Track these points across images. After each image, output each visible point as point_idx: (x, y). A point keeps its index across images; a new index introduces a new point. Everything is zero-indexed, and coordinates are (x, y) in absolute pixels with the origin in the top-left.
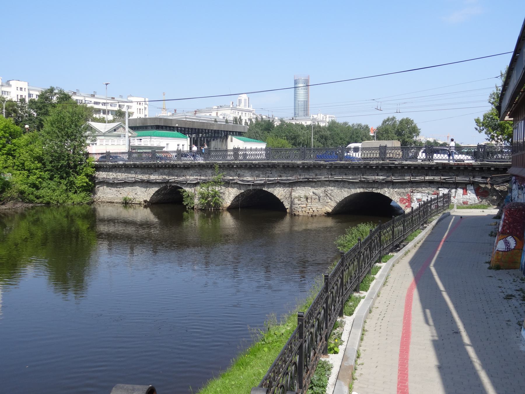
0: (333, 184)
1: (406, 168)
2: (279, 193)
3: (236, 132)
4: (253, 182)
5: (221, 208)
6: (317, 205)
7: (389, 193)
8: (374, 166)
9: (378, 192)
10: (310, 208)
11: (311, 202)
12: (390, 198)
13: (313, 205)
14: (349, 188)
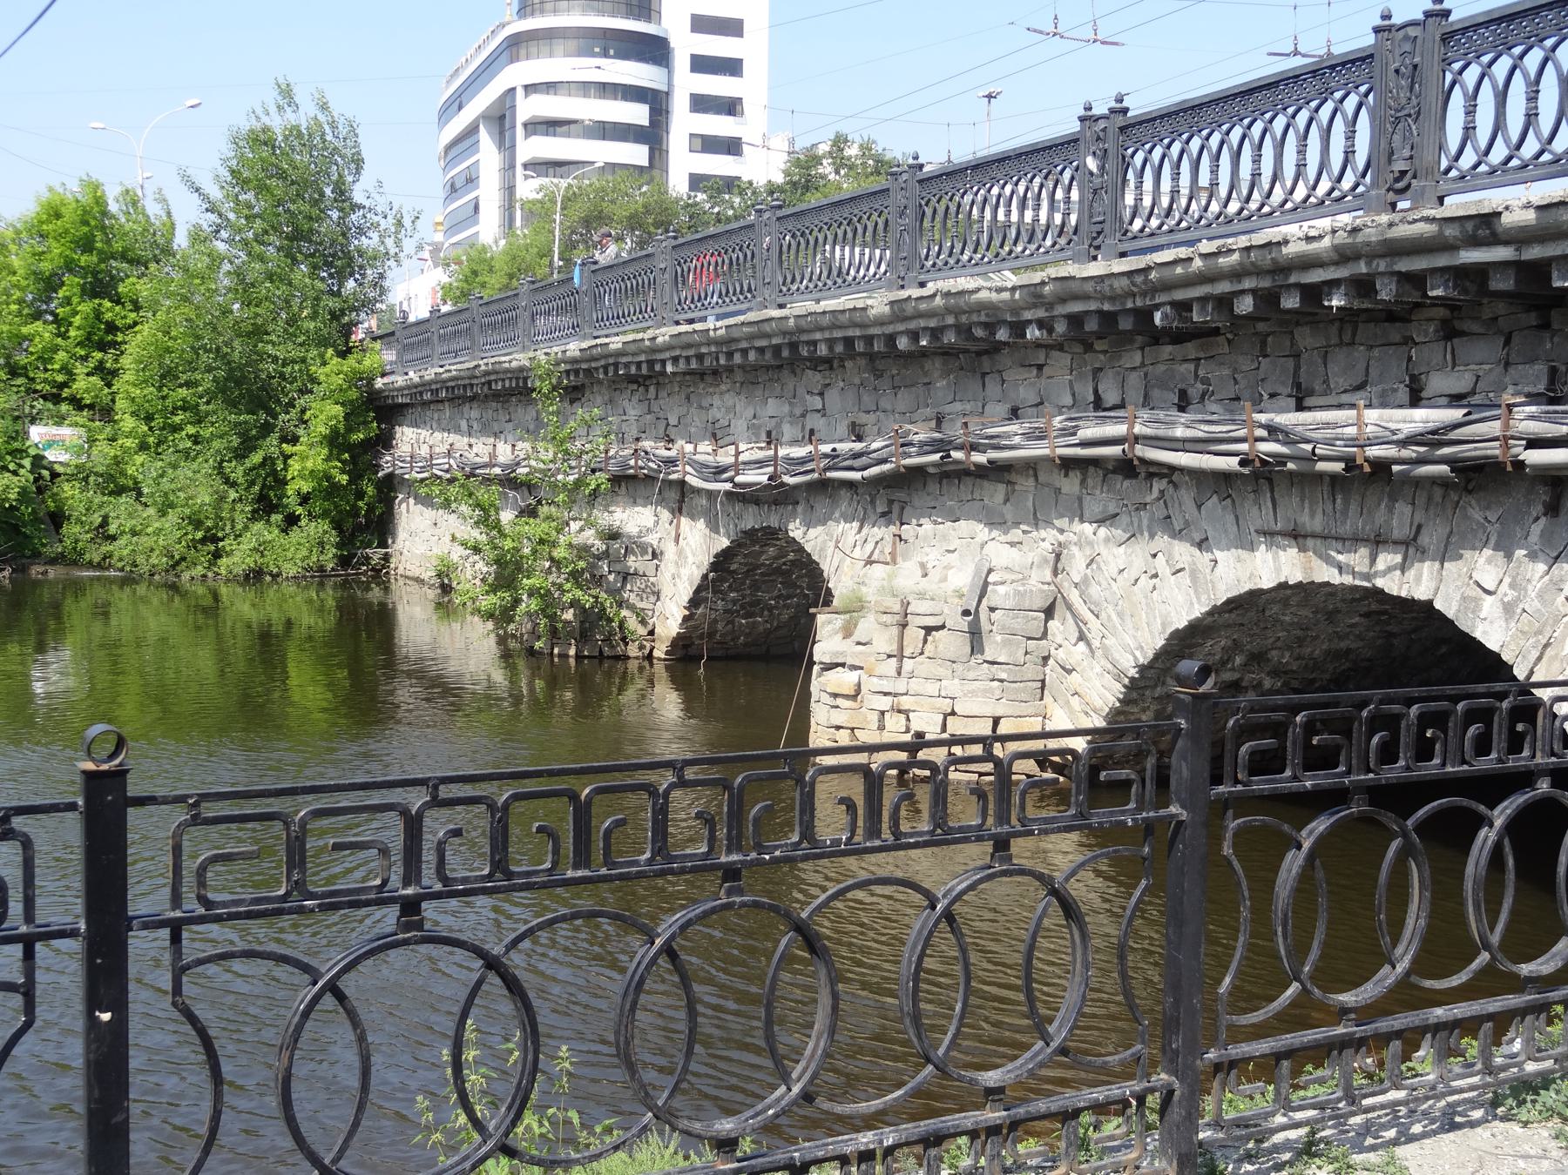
0: (1100, 500)
4: (731, 480)
5: (633, 651)
6: (952, 686)
7: (1508, 609)
8: (1333, 284)
9: (1421, 594)
10: (884, 703)
13: (915, 685)
14: (1202, 544)
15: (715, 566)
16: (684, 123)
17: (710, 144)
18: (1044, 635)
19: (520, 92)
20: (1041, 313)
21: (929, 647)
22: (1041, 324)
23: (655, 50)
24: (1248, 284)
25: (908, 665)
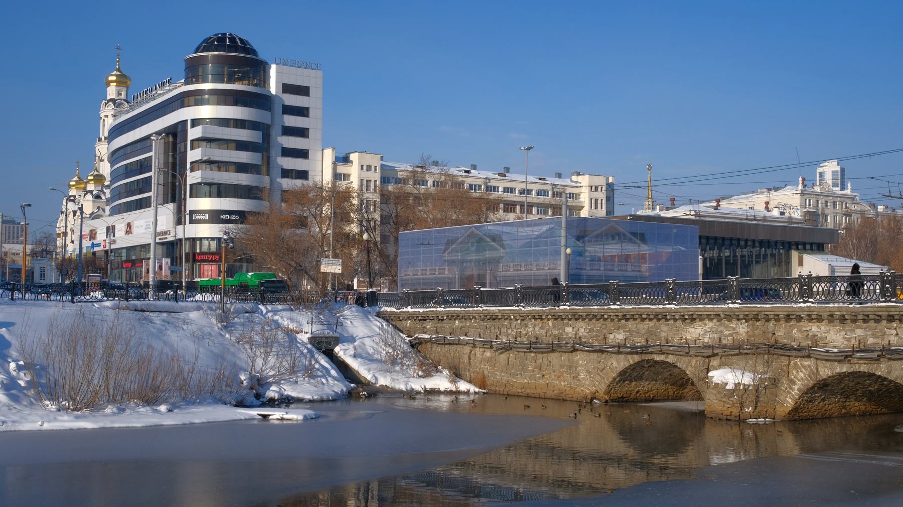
3: (811, 244)
23: (261, 101)
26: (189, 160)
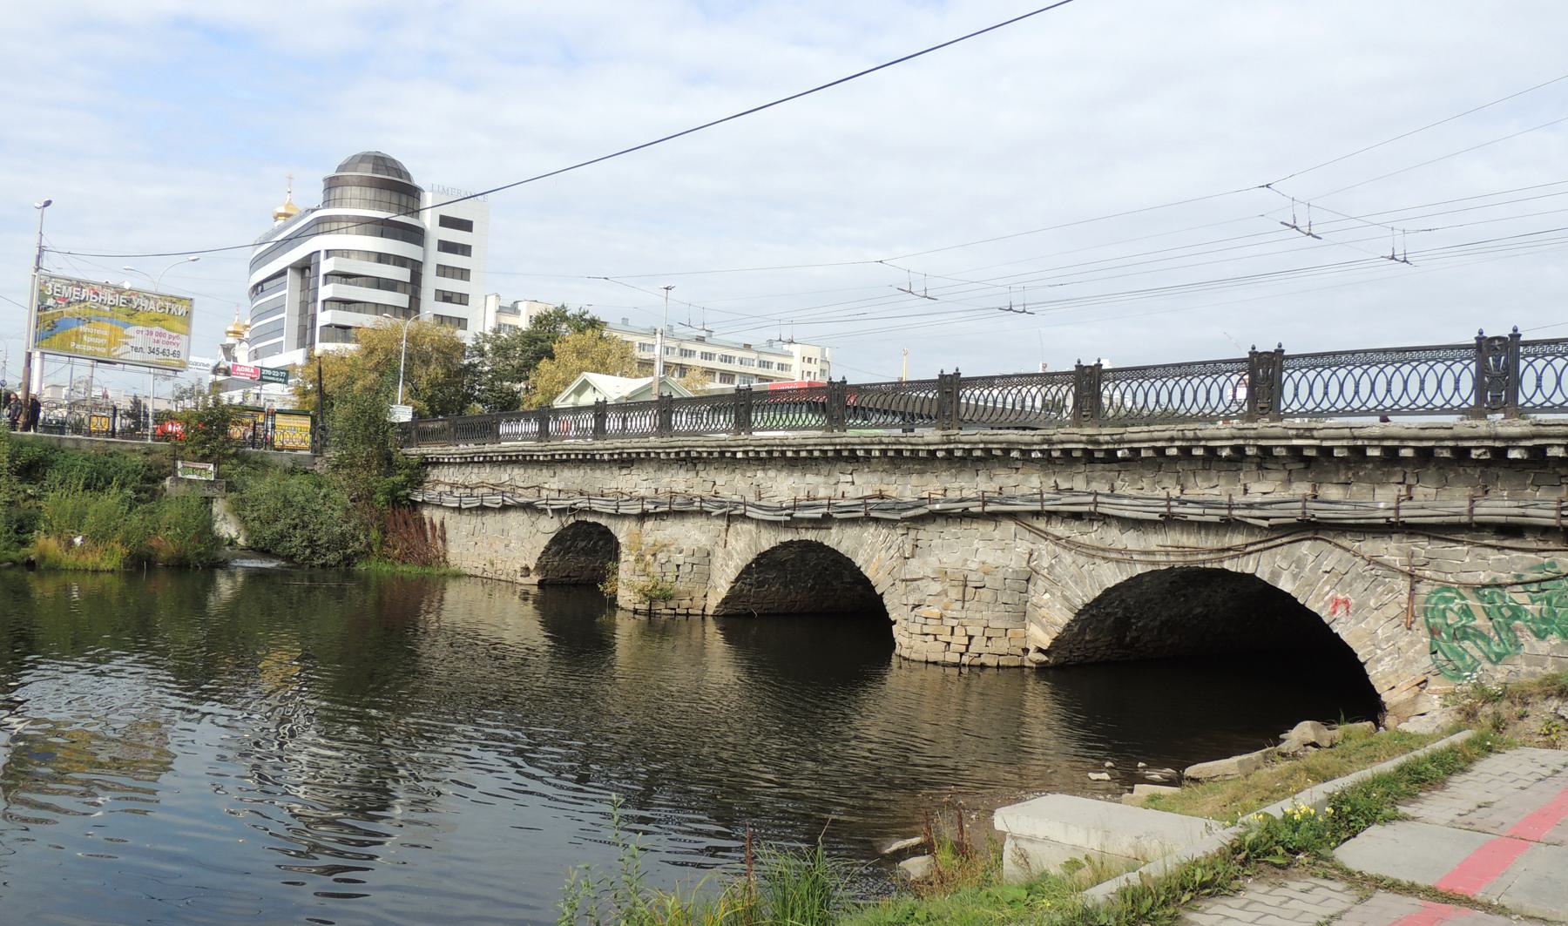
1: (1376, 453)
2: (872, 557)
7: (1295, 577)
8: (1222, 447)
9: (1249, 571)
10: (954, 623)
11: (964, 601)
12: (1301, 601)
15: (756, 561)
16: (432, 282)
17: (446, 297)
18: (1026, 592)
19: (323, 254)
20: (1045, 447)
21: (977, 596)
22: (1041, 451)
23: (415, 235)
24: (1178, 443)
25: (967, 605)
26: (322, 297)
